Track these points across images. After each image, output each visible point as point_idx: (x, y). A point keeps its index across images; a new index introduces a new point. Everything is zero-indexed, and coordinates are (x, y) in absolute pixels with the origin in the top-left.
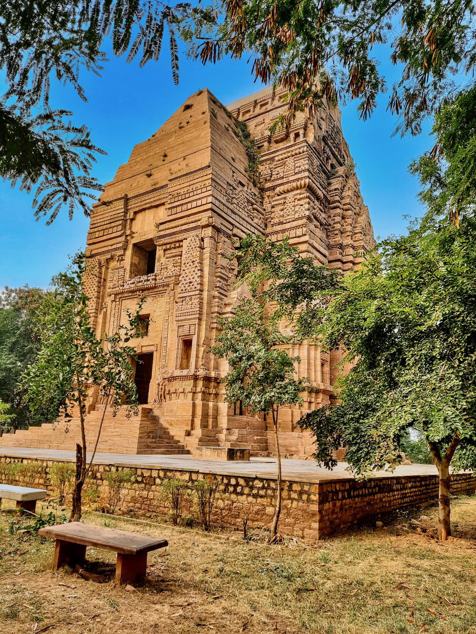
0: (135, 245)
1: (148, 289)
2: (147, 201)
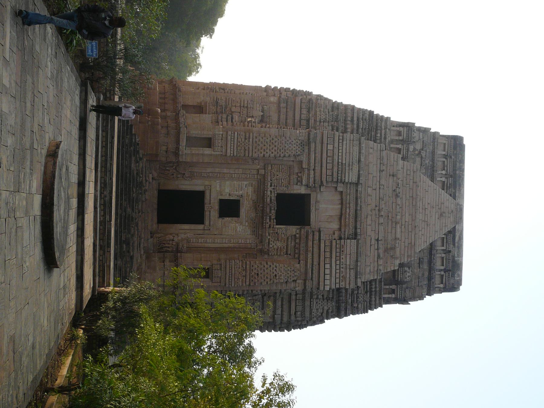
0: (309, 195)
1: (263, 217)
2: (348, 210)
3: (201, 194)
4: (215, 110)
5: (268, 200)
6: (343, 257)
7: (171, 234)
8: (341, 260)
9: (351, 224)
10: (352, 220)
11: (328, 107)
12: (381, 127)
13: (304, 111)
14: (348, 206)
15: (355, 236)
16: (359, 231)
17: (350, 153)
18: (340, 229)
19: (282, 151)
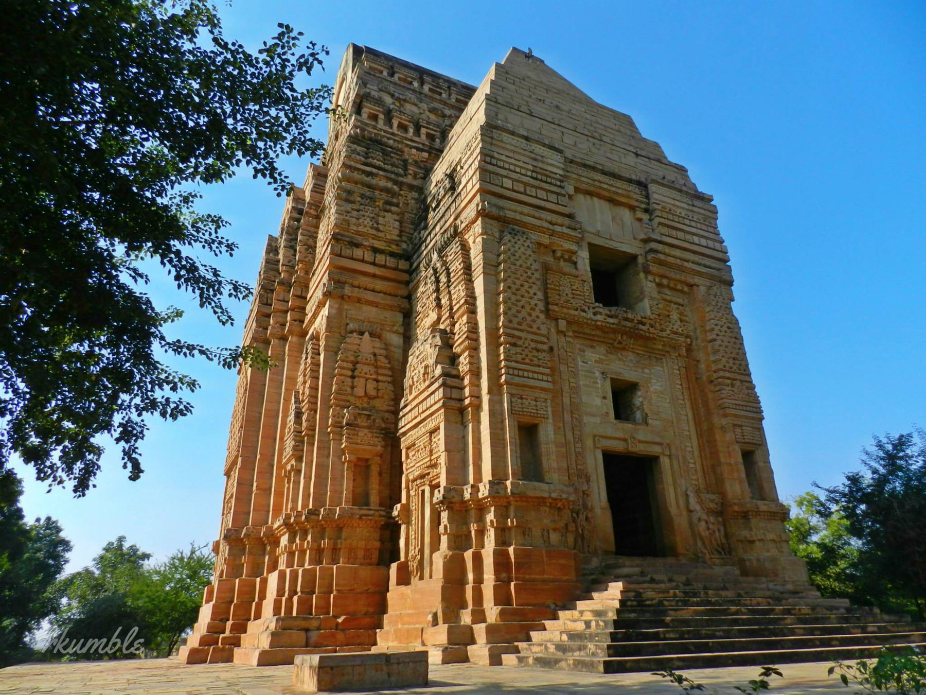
2: (605, 186)
3: (610, 458)
4: (366, 431)
5: (611, 320)
6: (678, 211)
7: (691, 524)
8: (683, 215)
9: (625, 187)
10: (619, 184)
11: (349, 209)
12: (375, 134)
13: (358, 253)
14: (597, 183)
15: (642, 185)
16: (634, 177)
17: (514, 152)
18: (632, 208)
19: (529, 274)
